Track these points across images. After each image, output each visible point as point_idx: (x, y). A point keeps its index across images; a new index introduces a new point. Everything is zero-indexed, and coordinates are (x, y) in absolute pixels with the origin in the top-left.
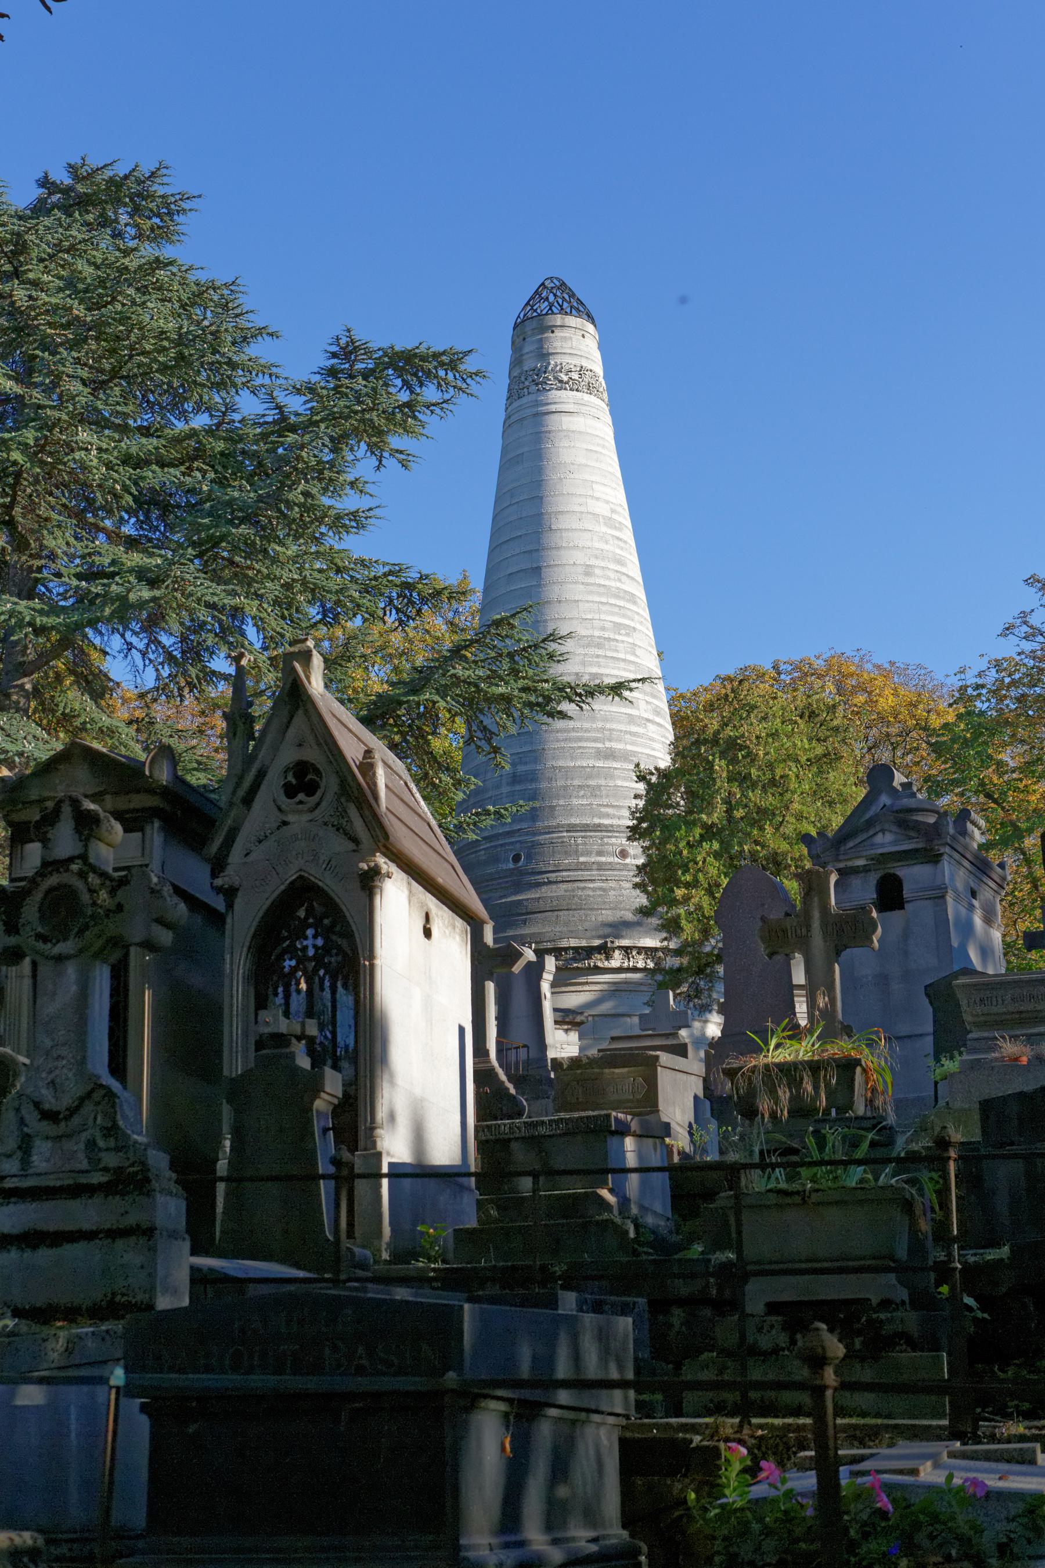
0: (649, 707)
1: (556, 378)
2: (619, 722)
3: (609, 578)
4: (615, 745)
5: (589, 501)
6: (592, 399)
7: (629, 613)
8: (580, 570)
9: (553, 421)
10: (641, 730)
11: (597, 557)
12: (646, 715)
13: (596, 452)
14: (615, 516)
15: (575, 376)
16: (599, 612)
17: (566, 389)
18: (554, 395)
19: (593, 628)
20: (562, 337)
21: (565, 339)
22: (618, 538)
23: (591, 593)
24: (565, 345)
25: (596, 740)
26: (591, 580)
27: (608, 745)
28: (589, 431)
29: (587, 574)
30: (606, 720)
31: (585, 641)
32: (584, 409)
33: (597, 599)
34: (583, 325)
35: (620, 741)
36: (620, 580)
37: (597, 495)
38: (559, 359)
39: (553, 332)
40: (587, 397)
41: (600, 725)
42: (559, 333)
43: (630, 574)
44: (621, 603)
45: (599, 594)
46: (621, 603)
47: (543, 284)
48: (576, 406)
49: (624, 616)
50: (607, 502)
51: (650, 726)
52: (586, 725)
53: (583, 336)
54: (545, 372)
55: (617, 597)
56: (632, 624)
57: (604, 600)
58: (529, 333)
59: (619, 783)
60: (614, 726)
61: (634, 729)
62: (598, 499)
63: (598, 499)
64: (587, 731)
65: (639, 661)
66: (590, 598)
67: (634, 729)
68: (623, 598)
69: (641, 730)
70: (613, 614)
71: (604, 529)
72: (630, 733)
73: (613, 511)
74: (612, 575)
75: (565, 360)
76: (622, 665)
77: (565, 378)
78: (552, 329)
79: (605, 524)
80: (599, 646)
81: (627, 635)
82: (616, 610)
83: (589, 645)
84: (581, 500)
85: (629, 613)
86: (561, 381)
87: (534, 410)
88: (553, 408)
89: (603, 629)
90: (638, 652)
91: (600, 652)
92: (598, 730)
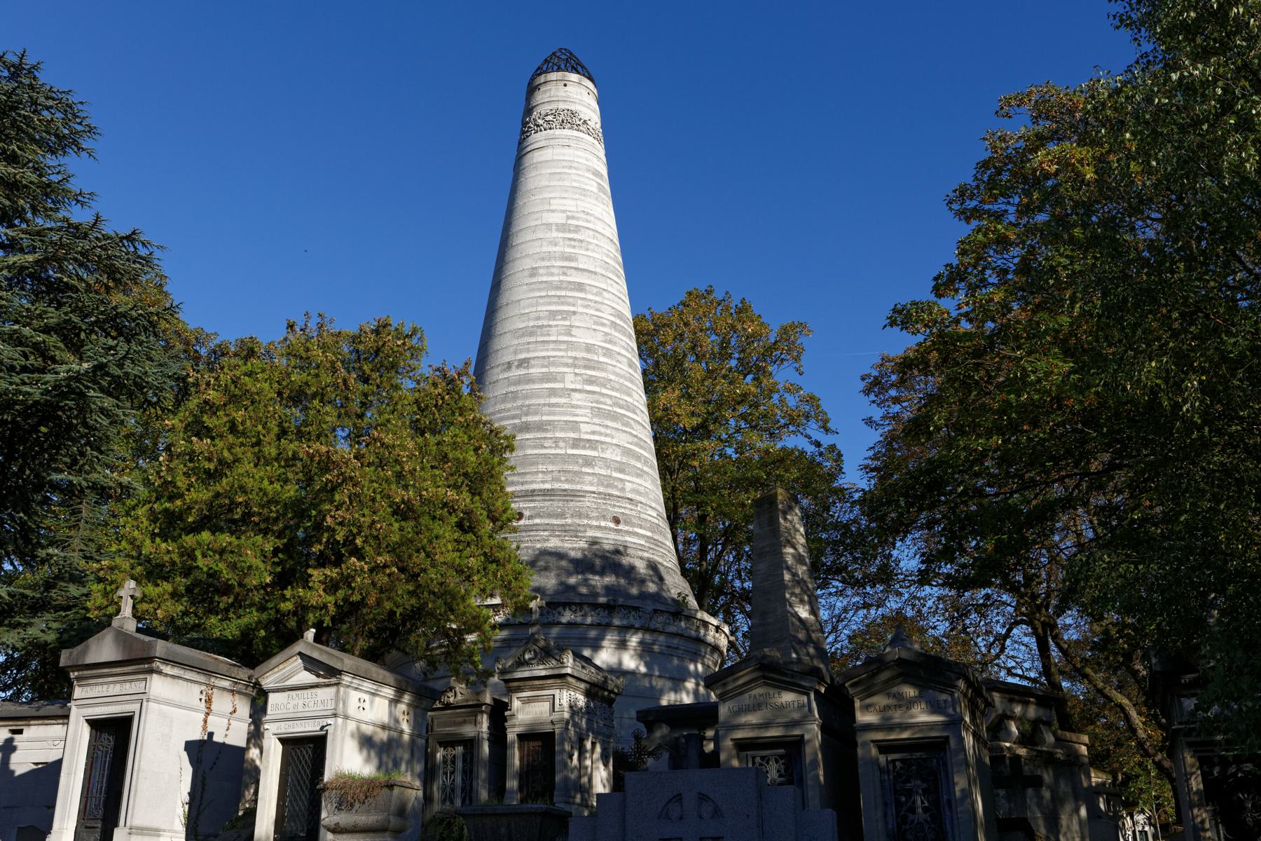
0: (579, 378)
2: (539, 397)
3: (552, 274)
4: (530, 418)
5: (545, 215)
6: (567, 132)
7: (571, 300)
8: (526, 273)
10: (562, 401)
11: (543, 259)
12: (573, 386)
14: (570, 222)
16: (537, 304)
19: (529, 320)
22: (570, 239)
23: (533, 290)
25: (514, 417)
26: (534, 280)
27: (524, 419)
29: (532, 275)
30: (526, 397)
31: (521, 332)
32: (552, 142)
33: (538, 294)
35: (536, 413)
36: (565, 274)
37: (553, 208)
41: (519, 403)
42: (543, 89)
43: (581, 266)
44: (563, 293)
45: (540, 290)
46: (563, 293)
47: (554, 54)
49: (563, 303)
50: (564, 211)
51: (577, 395)
52: (509, 406)
55: (558, 288)
56: (572, 309)
57: (543, 294)
59: (529, 452)
60: (533, 401)
61: (553, 400)
62: (553, 211)
63: (553, 211)
64: (509, 410)
65: (574, 339)
66: (531, 295)
67: (553, 400)
68: (565, 289)
69: (562, 401)
70: (550, 304)
71: (555, 234)
72: (549, 405)
73: (568, 218)
74: (555, 271)
76: (552, 346)
77: (540, 122)
79: (558, 230)
80: (532, 334)
81: (564, 319)
82: (555, 300)
83: (523, 335)
84: (536, 216)
85: (571, 300)
89: (538, 318)
90: (574, 331)
91: (533, 339)
92: (517, 408)
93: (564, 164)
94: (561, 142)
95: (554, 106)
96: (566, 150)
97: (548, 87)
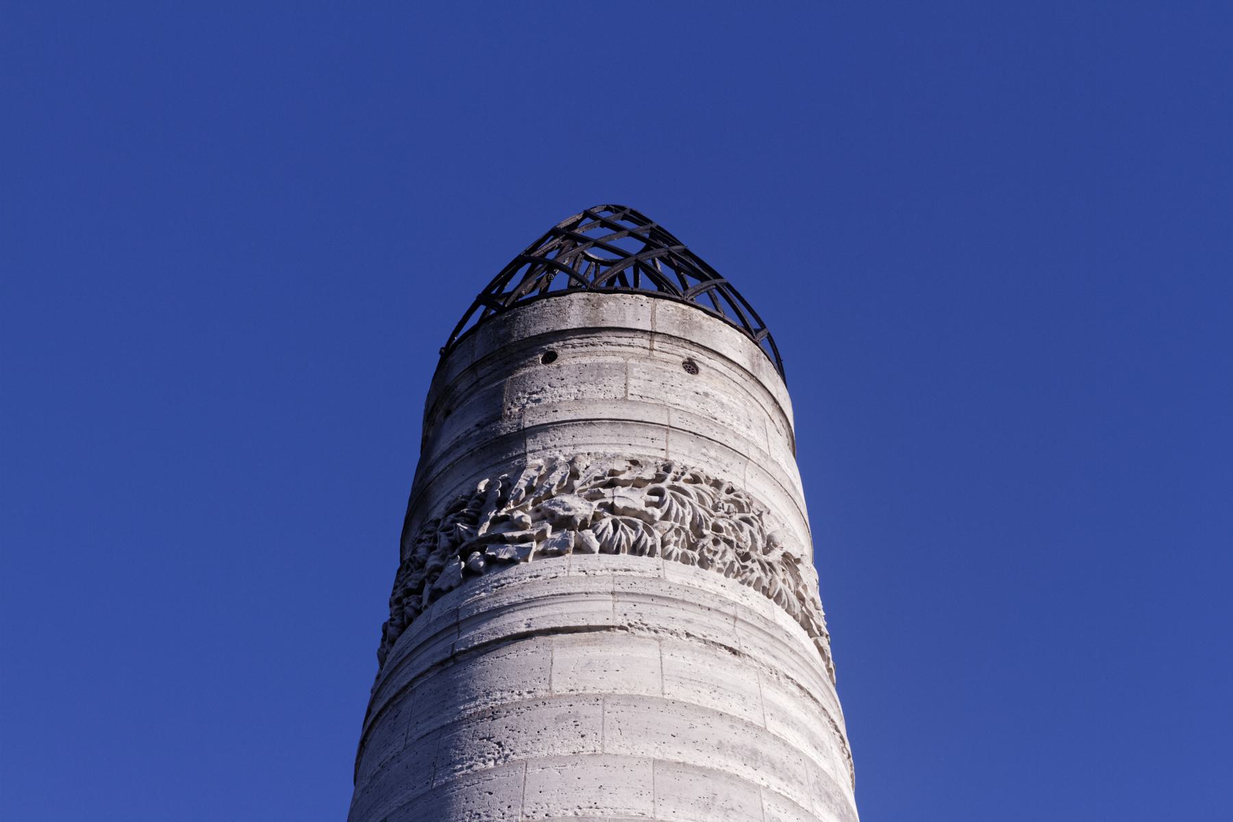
1: (542, 515)
6: (713, 582)
9: (508, 674)
13: (706, 772)
15: (636, 499)
17: (582, 548)
18: (533, 574)
20: (582, 368)
21: (599, 371)
24: (590, 391)
28: (675, 692)
32: (656, 615)
34: (687, 323)
38: (562, 447)
39: (550, 357)
40: (678, 574)
42: (571, 357)
48: (624, 606)
53: (691, 367)
54: (502, 503)
58: (463, 386)
75: (597, 451)
77: (580, 507)
78: (545, 347)
86: (564, 523)
87: (439, 651)
88: (517, 622)
93: (722, 731)
94: (703, 624)
95: (649, 449)
96: (725, 670)
97: (605, 354)
